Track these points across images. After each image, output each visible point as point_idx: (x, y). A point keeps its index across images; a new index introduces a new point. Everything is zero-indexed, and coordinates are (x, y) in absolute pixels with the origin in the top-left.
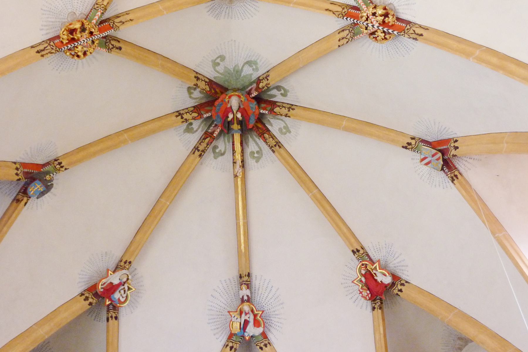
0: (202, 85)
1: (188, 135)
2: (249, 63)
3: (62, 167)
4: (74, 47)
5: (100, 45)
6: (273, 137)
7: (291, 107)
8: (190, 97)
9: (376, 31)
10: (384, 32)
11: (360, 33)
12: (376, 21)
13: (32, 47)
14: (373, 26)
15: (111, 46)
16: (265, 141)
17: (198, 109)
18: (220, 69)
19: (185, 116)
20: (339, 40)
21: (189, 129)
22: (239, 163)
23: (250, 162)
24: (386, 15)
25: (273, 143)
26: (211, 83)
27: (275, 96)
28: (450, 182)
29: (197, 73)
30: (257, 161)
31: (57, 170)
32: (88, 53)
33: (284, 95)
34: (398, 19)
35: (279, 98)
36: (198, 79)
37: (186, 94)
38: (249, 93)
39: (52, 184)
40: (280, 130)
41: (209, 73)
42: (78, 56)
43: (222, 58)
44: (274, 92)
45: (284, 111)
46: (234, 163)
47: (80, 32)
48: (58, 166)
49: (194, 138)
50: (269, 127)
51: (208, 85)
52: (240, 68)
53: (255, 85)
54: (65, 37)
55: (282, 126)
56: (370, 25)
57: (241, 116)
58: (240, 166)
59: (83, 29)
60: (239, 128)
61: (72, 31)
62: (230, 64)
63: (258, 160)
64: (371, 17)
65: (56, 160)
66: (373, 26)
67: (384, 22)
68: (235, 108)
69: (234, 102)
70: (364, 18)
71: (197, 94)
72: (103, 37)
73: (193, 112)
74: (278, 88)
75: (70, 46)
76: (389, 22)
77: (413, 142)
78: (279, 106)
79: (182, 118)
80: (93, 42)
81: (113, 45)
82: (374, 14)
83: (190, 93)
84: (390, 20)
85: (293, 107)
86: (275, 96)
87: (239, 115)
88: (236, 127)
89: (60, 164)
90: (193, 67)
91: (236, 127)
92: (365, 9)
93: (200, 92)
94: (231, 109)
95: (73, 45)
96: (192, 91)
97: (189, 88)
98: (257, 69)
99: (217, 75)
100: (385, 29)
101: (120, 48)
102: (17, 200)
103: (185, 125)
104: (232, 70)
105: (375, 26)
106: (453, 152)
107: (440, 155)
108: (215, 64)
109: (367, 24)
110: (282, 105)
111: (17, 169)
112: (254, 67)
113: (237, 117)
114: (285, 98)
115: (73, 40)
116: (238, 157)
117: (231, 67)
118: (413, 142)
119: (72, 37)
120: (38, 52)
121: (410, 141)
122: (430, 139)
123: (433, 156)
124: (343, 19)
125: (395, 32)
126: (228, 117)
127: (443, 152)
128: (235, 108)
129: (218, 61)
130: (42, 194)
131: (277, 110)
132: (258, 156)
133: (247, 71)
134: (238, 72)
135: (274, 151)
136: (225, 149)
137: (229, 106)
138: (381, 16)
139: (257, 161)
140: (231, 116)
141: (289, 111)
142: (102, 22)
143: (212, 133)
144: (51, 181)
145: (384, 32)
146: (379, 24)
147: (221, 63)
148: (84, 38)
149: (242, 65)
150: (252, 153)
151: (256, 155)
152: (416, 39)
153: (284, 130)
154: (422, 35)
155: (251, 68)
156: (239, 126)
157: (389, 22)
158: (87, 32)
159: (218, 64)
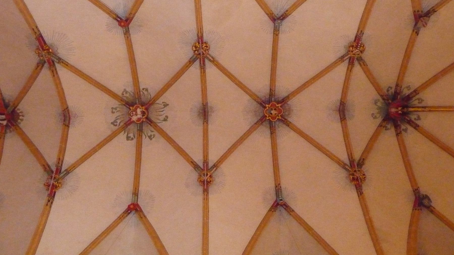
0: (384, 124)
1: (409, 131)
2: (376, 103)
3: (417, 189)
5: (361, 167)
6: (412, 93)
7: (397, 85)
8: (390, 129)
9: (360, 50)
10: (360, 47)
11: (361, 57)
12: (356, 51)
14: (357, 52)
15: (362, 163)
16: (413, 97)
17: (396, 126)
19: (398, 132)
20: (365, 65)
21: (406, 130)
22: (423, 109)
23: (423, 104)
24: (353, 46)
25: (414, 94)
26: (384, 120)
27: (392, 92)
28: (436, 13)
29: (379, 126)
30: (423, 101)
31: (419, 192)
32: (364, 173)
33: (391, 88)
34: (355, 41)
35: (393, 90)
38: (389, 103)
39: (425, 195)
40: (408, 90)
41: (379, 120)
42: (365, 178)
44: (390, 92)
45: (399, 88)
46: (423, 111)
47: (354, 176)
48: (417, 191)
49: (410, 129)
50: (407, 94)
54: (356, 182)
55: (406, 89)
56: (357, 53)
57: (400, 107)
58: (425, 109)
59: (353, 175)
60: (406, 108)
63: (422, 100)
64: (353, 53)
65: (414, 191)
66: (357, 52)
67: (355, 47)
68: (396, 110)
69: (393, 110)
70: (354, 56)
71: (389, 126)
72: (357, 167)
73: (397, 129)
74: (388, 91)
76: (356, 45)
77: (415, 31)
78: (397, 90)
79: (399, 133)
80: (359, 171)
81: (362, 162)
82: (352, 52)
84: (355, 44)
85: (397, 84)
86: (392, 92)
87: (400, 108)
88: (405, 110)
89: (416, 190)
91: (405, 110)
92: (350, 55)
93: (388, 125)
94: (397, 112)
95: (359, 180)
96: (387, 128)
97: (386, 130)
98: (379, 100)
100: (359, 47)
101: (364, 159)
102: (432, 212)
103: (403, 132)
104: (379, 110)
106: (420, 12)
107: (422, 18)
109: (357, 54)
110: (396, 89)
111: (416, 209)
112: (378, 101)
113: (401, 109)
114: (393, 88)
116: (420, 109)
117: (377, 111)
118: (415, 31)
119: (355, 180)
120: (361, 195)
121: (415, 32)
122: (414, 24)
123: (422, 21)
124: (354, 64)
126: (400, 113)
127: (421, 16)
128: (396, 110)
130: (429, 199)
131: (398, 91)
132: (421, 101)
133: (379, 104)
134: (379, 108)
135: (418, 93)
136: (416, 115)
137: (395, 112)
138: (353, 48)
139: (423, 101)
140: (400, 112)
141: (399, 86)
142: (351, 167)
143: (408, 120)
144: (423, 195)
145: (360, 47)
146: (357, 49)
147: (375, 115)
148: (357, 175)
150: (419, 103)
151: (420, 101)
152: (363, 33)
153: (409, 88)
154: (361, 31)
156: (405, 108)
157: (356, 45)
158: (354, 173)
159: (376, 116)
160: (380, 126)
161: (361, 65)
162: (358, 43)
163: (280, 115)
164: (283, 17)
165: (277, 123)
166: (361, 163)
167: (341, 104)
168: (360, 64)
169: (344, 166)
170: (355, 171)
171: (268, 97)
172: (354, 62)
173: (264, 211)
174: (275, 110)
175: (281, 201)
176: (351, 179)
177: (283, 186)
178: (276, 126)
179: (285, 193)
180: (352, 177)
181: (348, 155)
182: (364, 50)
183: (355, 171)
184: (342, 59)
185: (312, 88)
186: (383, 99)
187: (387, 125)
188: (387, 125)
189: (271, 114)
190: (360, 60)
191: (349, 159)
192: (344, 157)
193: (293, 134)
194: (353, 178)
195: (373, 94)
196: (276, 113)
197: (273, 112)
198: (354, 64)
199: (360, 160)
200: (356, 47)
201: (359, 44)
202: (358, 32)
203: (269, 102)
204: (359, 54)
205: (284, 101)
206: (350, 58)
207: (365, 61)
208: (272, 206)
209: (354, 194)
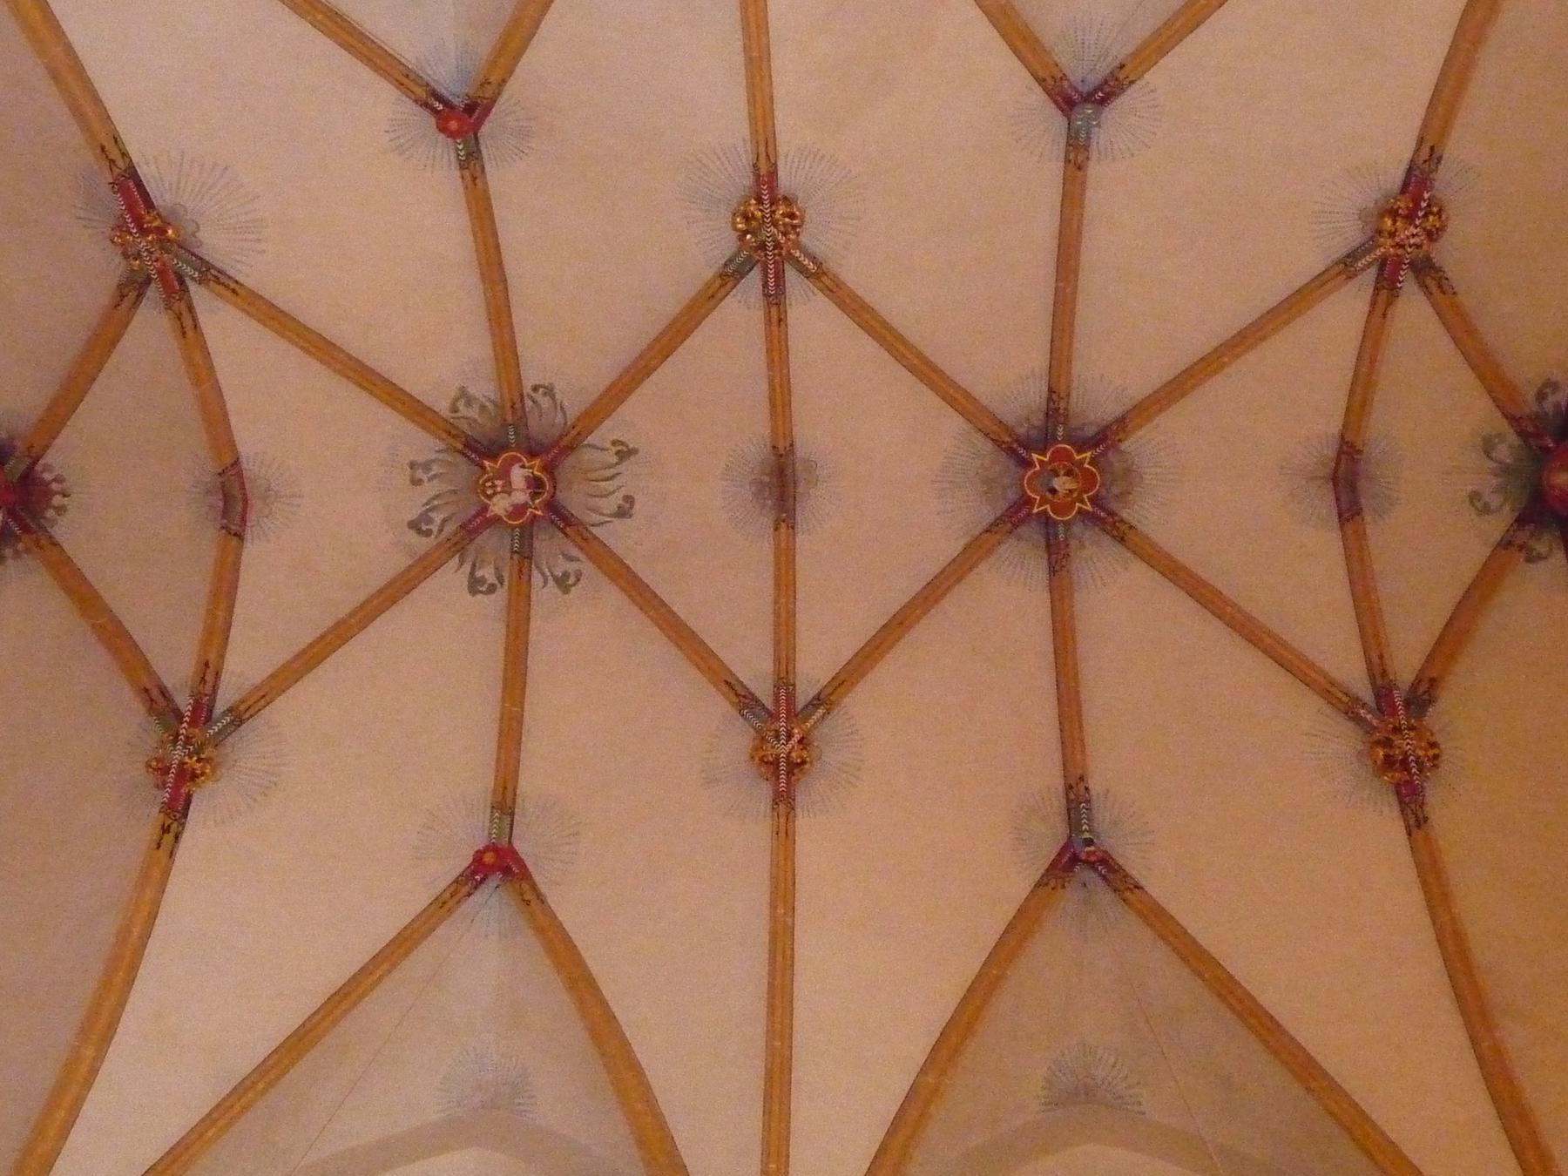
0: (1522, 537)
2: (1488, 448)
4: (1416, 763)
9: (1424, 229)
10: (1426, 216)
11: (1428, 259)
12: (1406, 232)
13: (1409, 834)
14: (1413, 236)
15: (1426, 697)
18: (1495, 501)
20: (1444, 293)
24: (1394, 214)
26: (1521, 521)
32: (1432, 739)
36: (1510, 543)
37: (1541, 565)
38: (1545, 450)
42: (1436, 757)
43: (1474, 497)
44: (1548, 406)
47: (1391, 747)
51: (1524, 526)
52: (1495, 465)
53: (1532, 441)
56: (1412, 241)
59: (1387, 743)
61: (1389, 762)
62: (1488, 484)
64: (1397, 240)
66: (1413, 236)
70: (1400, 252)
71: (1541, 547)
74: (1541, 397)
75: (1414, 770)
76: (1408, 208)
80: (1412, 728)
82: (1392, 235)
83: (1540, 558)
84: (1403, 205)
90: (1487, 551)
92: (1383, 250)
95: (1413, 764)
96: (1534, 553)
97: (1529, 560)
99: (1507, 508)
100: (1420, 214)
105: (1415, 232)
108: (1486, 510)
115: (1404, 763)
119: (1397, 765)
120: (1419, 826)
125: (1426, 196)
129: (1479, 504)
133: (1503, 452)
134: (1505, 470)
138: (1395, 222)
145: (1426, 216)
146: (1410, 224)
148: (1404, 744)
149: (1491, 462)
152: (1439, 159)
154: (1432, 148)
155: (1499, 447)
157: (1408, 208)
160: (1505, 544)
161: (1429, 294)
162: (1417, 200)
163: (1049, 510)
164: (1106, 92)
165: (1077, 529)
166: (1423, 695)
167: (1340, 453)
168: (1424, 286)
169: (1349, 708)
170: (1397, 730)
171: (1038, 419)
172: (1401, 279)
173: (1018, 884)
174: (1069, 473)
175: (1089, 846)
176: (1379, 762)
177: (1096, 785)
178: (1073, 543)
179: (1103, 816)
180: (1381, 753)
181: (1369, 662)
182: (1442, 229)
183: (1397, 730)
184: (1347, 265)
185: (1218, 390)
186: (1521, 433)
187: (1532, 543)
188: (1532, 543)
189: (1053, 491)
190: (1426, 270)
191: (1372, 677)
192: (1351, 672)
193: (1139, 573)
194: (1387, 756)
195: (1480, 413)
196: (1073, 486)
197: (1062, 484)
198: (1399, 285)
199: (1418, 681)
200: (1410, 218)
201: (1424, 205)
202: (1417, 150)
203: (1045, 440)
204: (1418, 246)
205: (1106, 438)
206: (1383, 263)
207: (1449, 275)
208: (1053, 865)
209: (1386, 823)
